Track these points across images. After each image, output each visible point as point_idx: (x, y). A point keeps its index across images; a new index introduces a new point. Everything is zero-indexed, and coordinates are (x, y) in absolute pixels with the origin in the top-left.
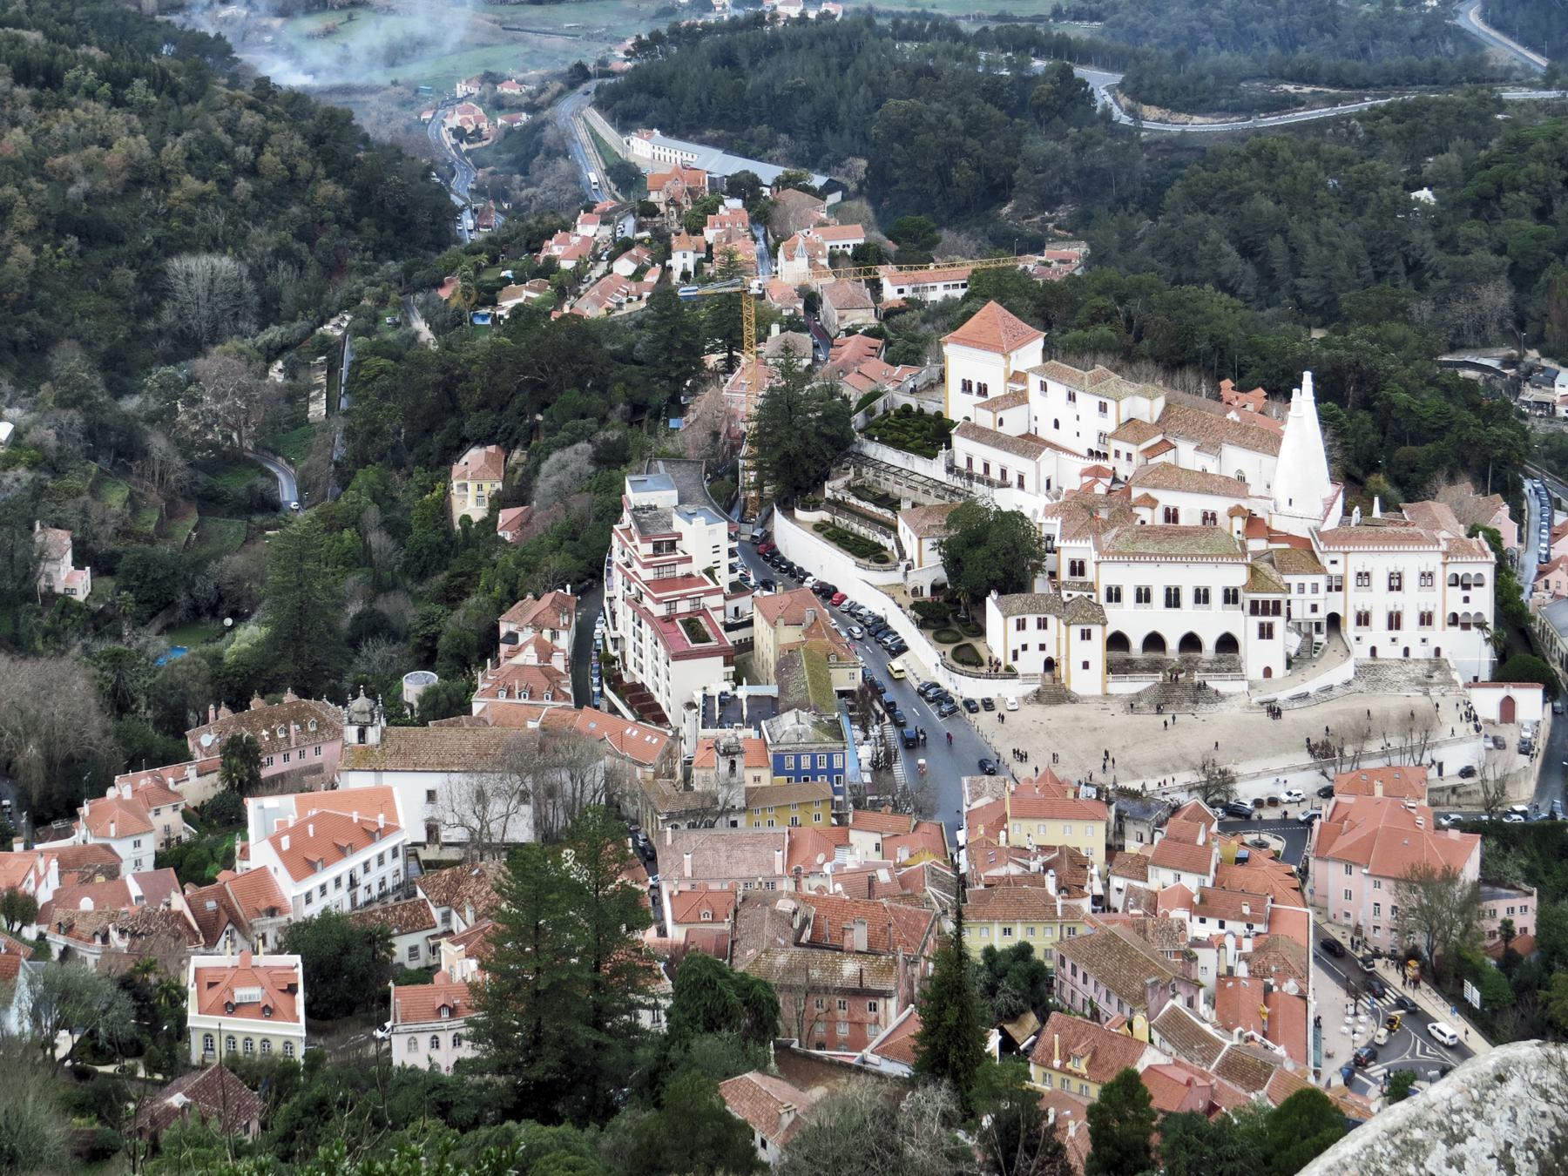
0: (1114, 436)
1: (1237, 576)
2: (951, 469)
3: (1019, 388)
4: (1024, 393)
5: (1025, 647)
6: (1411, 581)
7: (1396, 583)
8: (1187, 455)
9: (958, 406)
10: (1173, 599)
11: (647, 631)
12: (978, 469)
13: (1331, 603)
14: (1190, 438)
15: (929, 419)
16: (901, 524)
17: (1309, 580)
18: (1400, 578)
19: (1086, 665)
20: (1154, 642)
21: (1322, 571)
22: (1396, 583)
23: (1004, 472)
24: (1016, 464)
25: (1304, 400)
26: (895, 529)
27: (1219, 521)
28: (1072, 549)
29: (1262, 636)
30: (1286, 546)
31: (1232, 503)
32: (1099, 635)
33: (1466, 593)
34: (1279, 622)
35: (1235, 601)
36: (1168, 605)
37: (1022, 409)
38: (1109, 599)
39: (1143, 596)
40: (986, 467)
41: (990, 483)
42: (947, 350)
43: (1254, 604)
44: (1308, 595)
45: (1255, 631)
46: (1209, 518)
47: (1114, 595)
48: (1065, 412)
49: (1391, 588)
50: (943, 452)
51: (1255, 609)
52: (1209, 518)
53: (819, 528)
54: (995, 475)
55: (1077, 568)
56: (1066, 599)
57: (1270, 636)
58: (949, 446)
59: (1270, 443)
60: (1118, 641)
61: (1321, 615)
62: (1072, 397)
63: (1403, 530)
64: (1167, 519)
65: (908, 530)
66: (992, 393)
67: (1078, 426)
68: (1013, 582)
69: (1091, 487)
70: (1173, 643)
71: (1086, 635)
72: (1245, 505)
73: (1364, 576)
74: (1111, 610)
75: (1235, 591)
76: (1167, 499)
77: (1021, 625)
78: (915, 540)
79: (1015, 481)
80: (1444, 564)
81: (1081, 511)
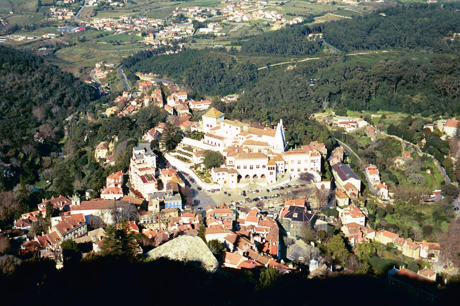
0: (240, 134)
3: (218, 125)
4: (220, 126)
12: (210, 143)
24: (218, 141)
25: (280, 124)
26: (192, 156)
27: (262, 152)
31: (265, 147)
35: (265, 167)
50: (202, 140)
58: (204, 138)
59: (273, 135)
62: (230, 127)
63: (301, 151)
66: (213, 127)
68: (217, 166)
69: (234, 146)
74: (238, 170)
77: (219, 174)
79: (218, 145)
81: (232, 150)
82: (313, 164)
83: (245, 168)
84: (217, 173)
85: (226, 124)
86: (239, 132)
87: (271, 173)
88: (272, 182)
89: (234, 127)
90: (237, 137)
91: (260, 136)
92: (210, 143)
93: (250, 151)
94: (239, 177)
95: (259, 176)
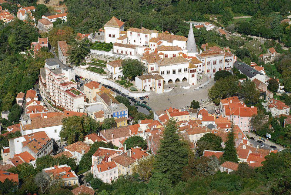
1: (187, 66)
2: (113, 53)
5: (146, 86)
6: (218, 62)
7: (215, 63)
8: (165, 43)
9: (108, 40)
10: (174, 72)
11: (63, 94)
12: (120, 52)
13: (202, 68)
16: (107, 65)
17: (199, 65)
18: (215, 62)
20: (170, 81)
21: (202, 63)
22: (215, 63)
23: (126, 52)
24: (129, 50)
26: (106, 67)
28: (150, 66)
29: (192, 77)
30: (191, 59)
31: (179, 51)
33: (228, 63)
34: (196, 74)
35: (186, 71)
37: (127, 39)
38: (162, 74)
39: (168, 72)
40: (122, 52)
41: (124, 55)
42: (105, 28)
43: (191, 71)
44: (199, 68)
46: (174, 56)
47: (163, 73)
49: (214, 64)
52: (174, 56)
53: (87, 69)
54: (124, 53)
55: (152, 69)
56: (153, 75)
57: (194, 77)
61: (201, 71)
62: (139, 35)
64: (165, 57)
65: (110, 66)
70: (174, 81)
72: (182, 51)
73: (209, 63)
74: (162, 76)
76: (165, 52)
77: (145, 82)
78: (113, 68)
80: (224, 58)
82: (227, 63)
83: (168, 72)
84: (144, 81)
85: (132, 32)
87: (193, 76)
88: (193, 84)
89: (143, 35)
91: (171, 41)
92: (120, 52)
93: (166, 56)
95: (181, 80)
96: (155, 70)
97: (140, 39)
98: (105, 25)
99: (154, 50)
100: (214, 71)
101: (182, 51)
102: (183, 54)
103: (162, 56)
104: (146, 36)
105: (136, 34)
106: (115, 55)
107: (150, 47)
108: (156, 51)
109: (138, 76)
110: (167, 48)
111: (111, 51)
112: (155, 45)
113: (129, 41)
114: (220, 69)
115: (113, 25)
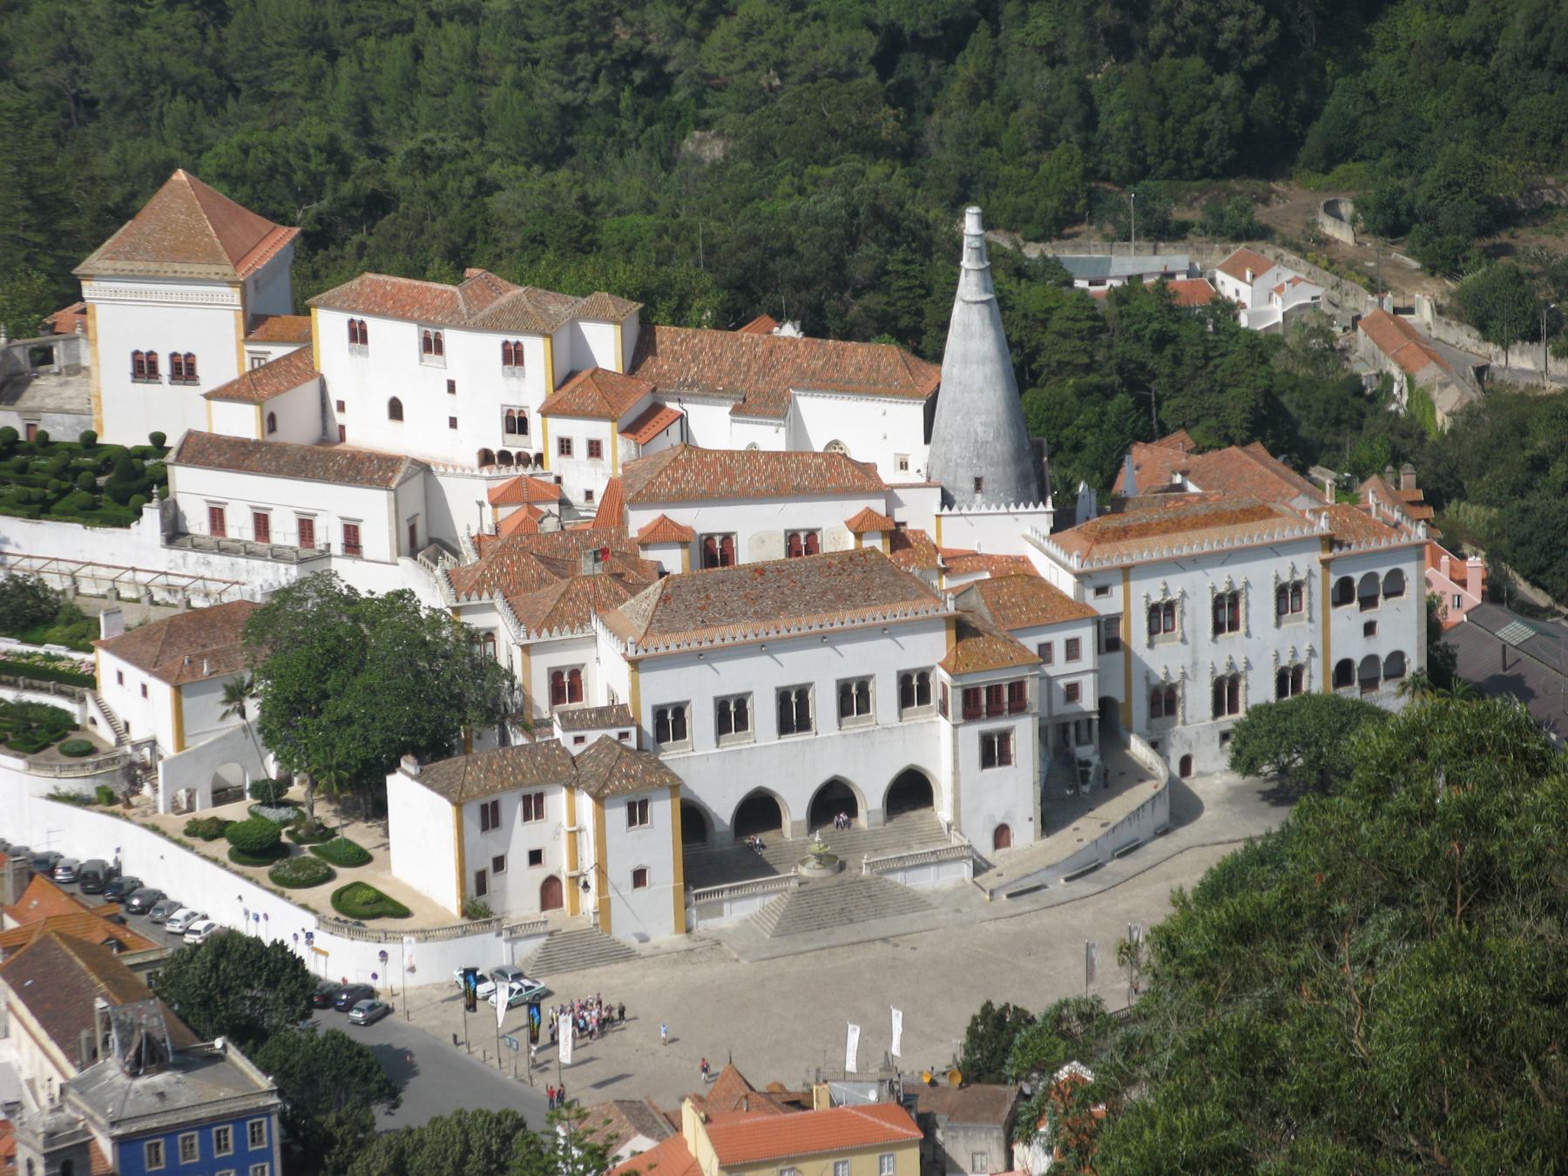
0: (546, 412)
5: (499, 863)
6: (1259, 606)
9: (127, 417)
10: (793, 712)
12: (239, 527)
14: (707, 392)
15: (70, 449)
16: (106, 664)
19: (639, 877)
23: (306, 528)
24: (331, 504)
31: (855, 507)
32: (663, 813)
33: (1369, 614)
35: (924, 698)
36: (785, 727)
37: (312, 387)
40: (262, 523)
45: (973, 751)
47: (671, 722)
48: (417, 380)
49: (1218, 628)
51: (972, 706)
54: (284, 533)
55: (566, 685)
57: (1005, 759)
58: (164, 495)
60: (693, 819)
61: (1088, 702)
62: (432, 345)
65: (135, 676)
67: (452, 406)
70: (795, 809)
71: (637, 813)
73: (1161, 615)
74: (671, 754)
75: (924, 676)
77: (491, 817)
78: (162, 691)
79: (337, 542)
82: (1349, 618)
83: (731, 715)
85: (374, 325)
86: (532, 387)
88: (1001, 835)
89: (470, 351)
90: (515, 445)
92: (239, 527)
93: (714, 553)
94: (693, 819)
96: (595, 696)
97: (451, 387)
98: (94, 261)
99: (597, 500)
100: (1225, 692)
101: (879, 506)
102: (897, 537)
103: (673, 560)
104: (513, 356)
105: (407, 334)
106: (193, 556)
107: (554, 462)
108: (618, 498)
109: (408, 764)
110: (727, 472)
111: (151, 516)
112: (606, 449)
113: (339, 418)
114: (1288, 679)
115: (173, 261)
